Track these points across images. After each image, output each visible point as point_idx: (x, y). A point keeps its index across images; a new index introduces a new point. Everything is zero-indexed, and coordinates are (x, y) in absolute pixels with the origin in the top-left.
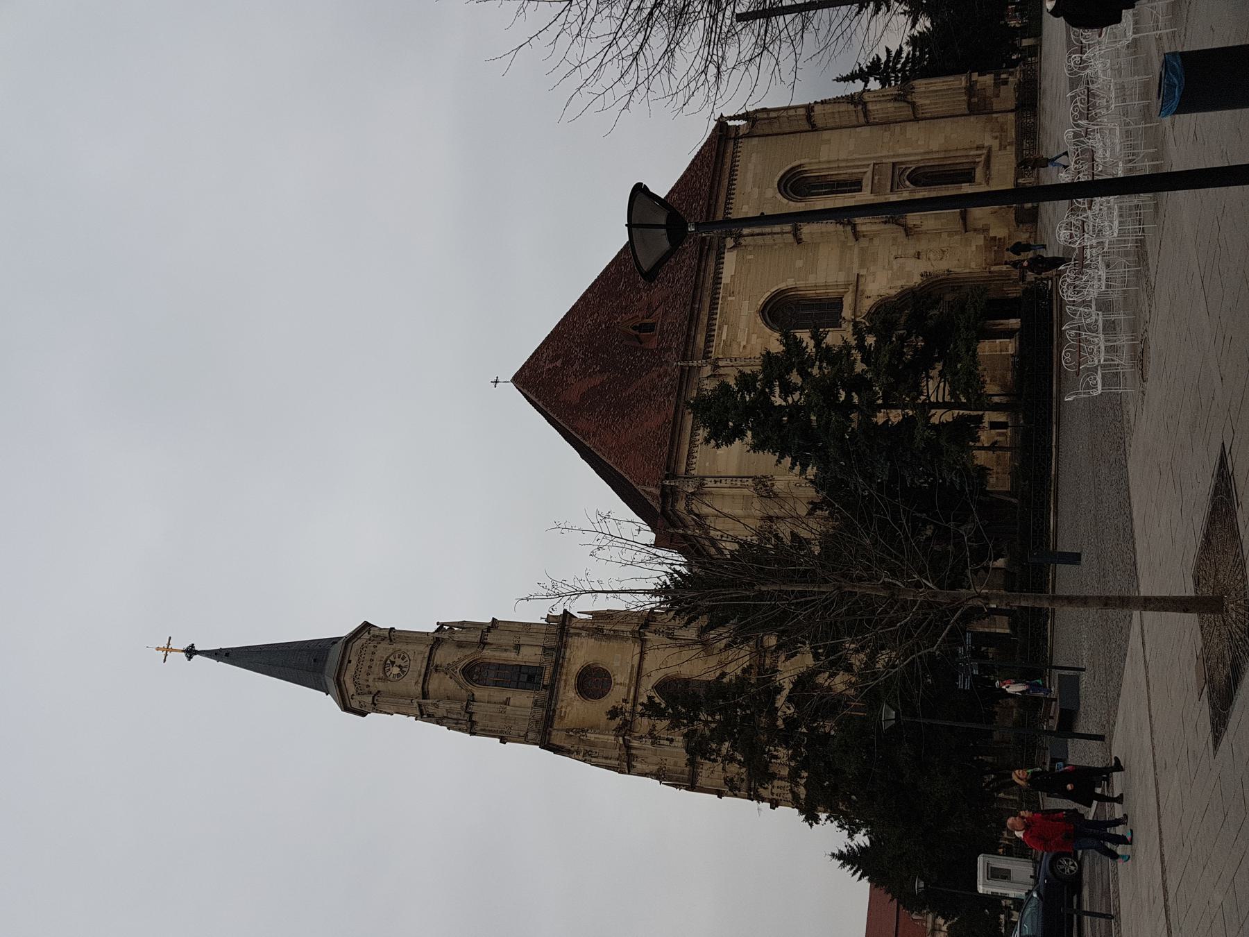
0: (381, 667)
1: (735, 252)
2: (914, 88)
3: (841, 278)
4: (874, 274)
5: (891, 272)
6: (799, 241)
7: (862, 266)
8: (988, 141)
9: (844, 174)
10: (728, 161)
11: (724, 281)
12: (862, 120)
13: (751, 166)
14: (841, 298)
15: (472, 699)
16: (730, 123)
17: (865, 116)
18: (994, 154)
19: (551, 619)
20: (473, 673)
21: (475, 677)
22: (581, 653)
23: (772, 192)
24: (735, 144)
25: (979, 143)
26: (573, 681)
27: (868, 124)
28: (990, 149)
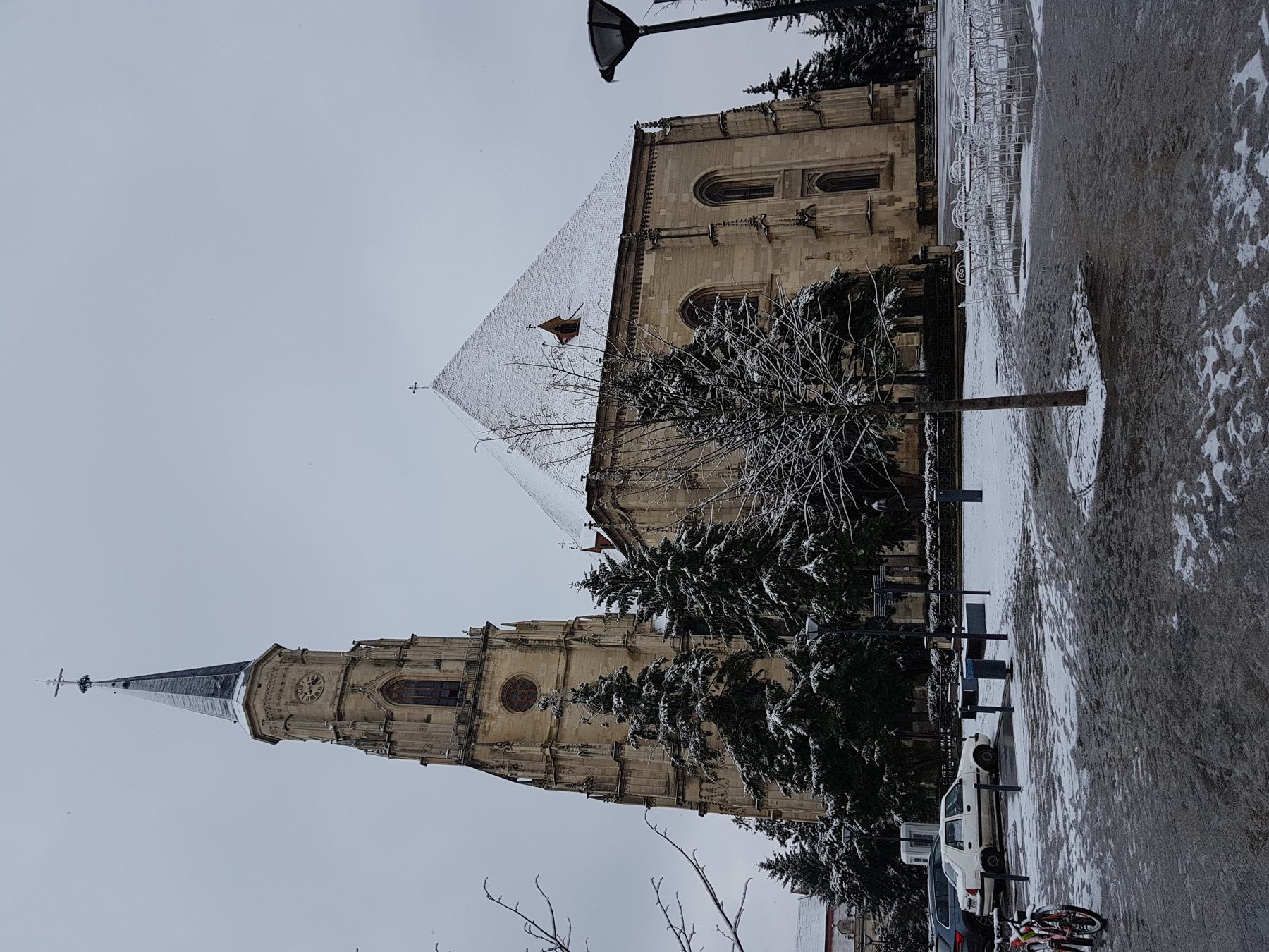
0: (294, 689)
1: (654, 253)
2: (820, 98)
3: (756, 278)
4: (787, 274)
6: (715, 243)
7: (775, 267)
8: (891, 149)
9: (757, 179)
10: (645, 166)
11: (644, 282)
12: (772, 129)
13: (667, 172)
14: (757, 298)
15: (390, 717)
16: (646, 130)
17: (775, 125)
18: (896, 160)
19: (473, 632)
20: (393, 691)
21: (394, 696)
22: (504, 666)
23: (688, 196)
24: (651, 151)
25: (882, 150)
26: (497, 693)
27: (777, 132)
28: (892, 156)
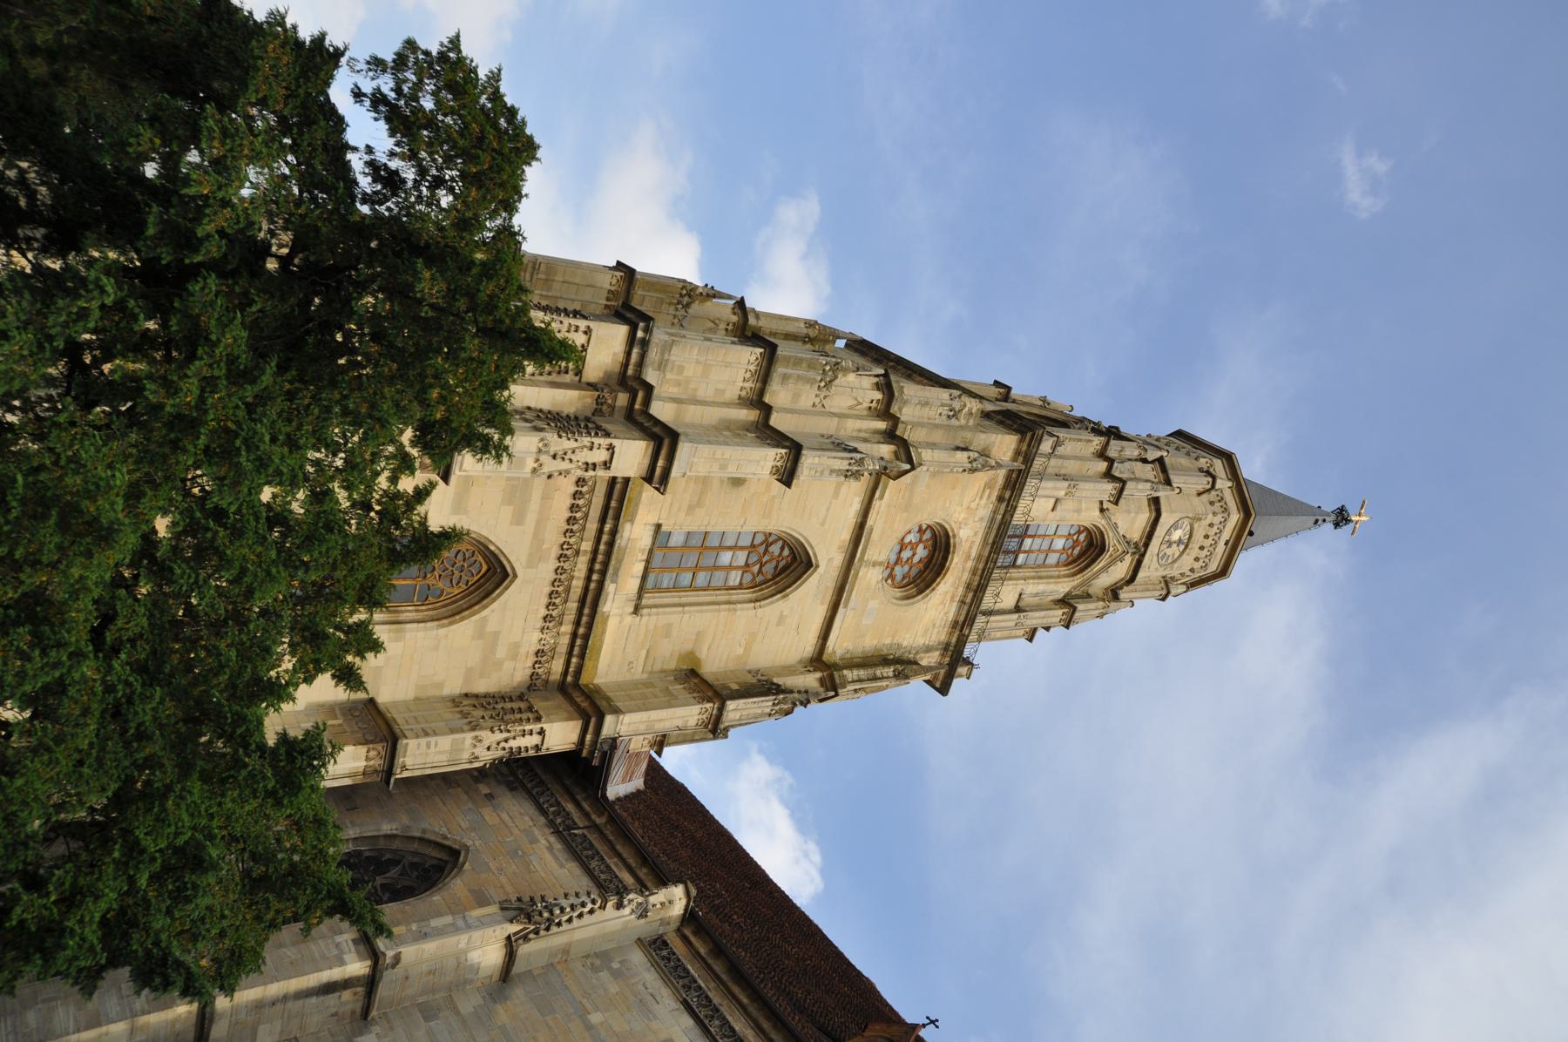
26: (955, 560)
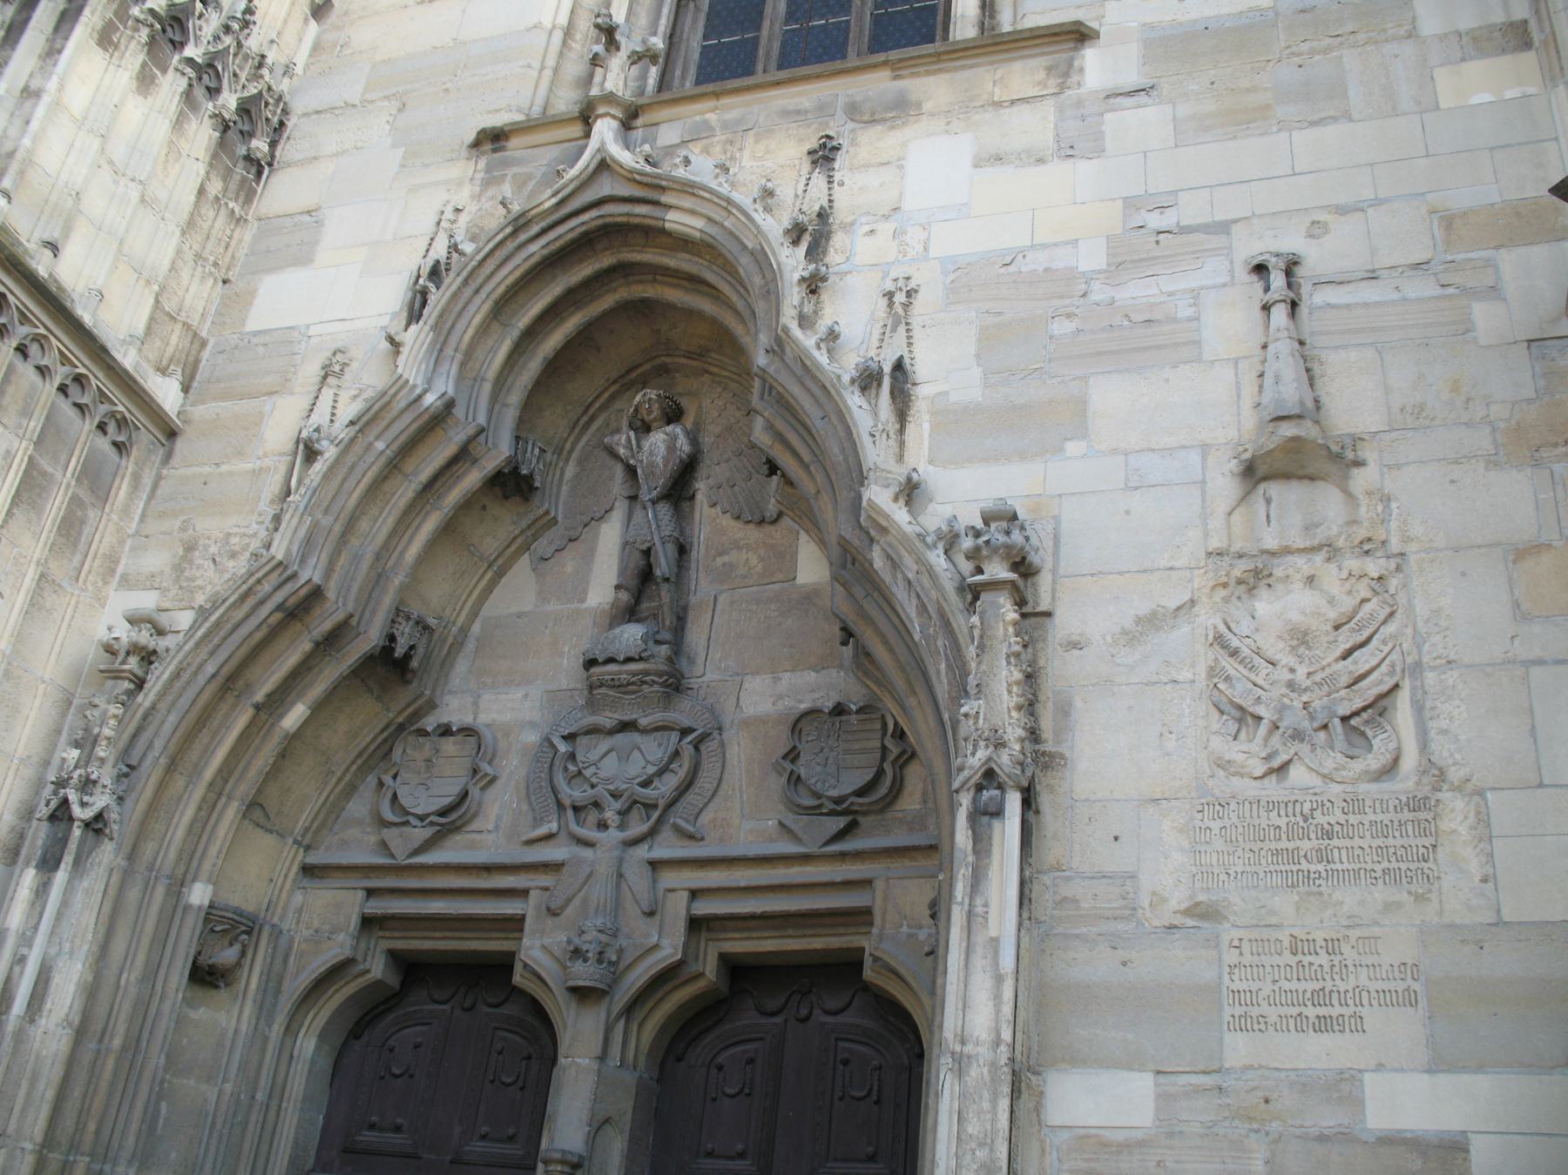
5: (1091, 258)
